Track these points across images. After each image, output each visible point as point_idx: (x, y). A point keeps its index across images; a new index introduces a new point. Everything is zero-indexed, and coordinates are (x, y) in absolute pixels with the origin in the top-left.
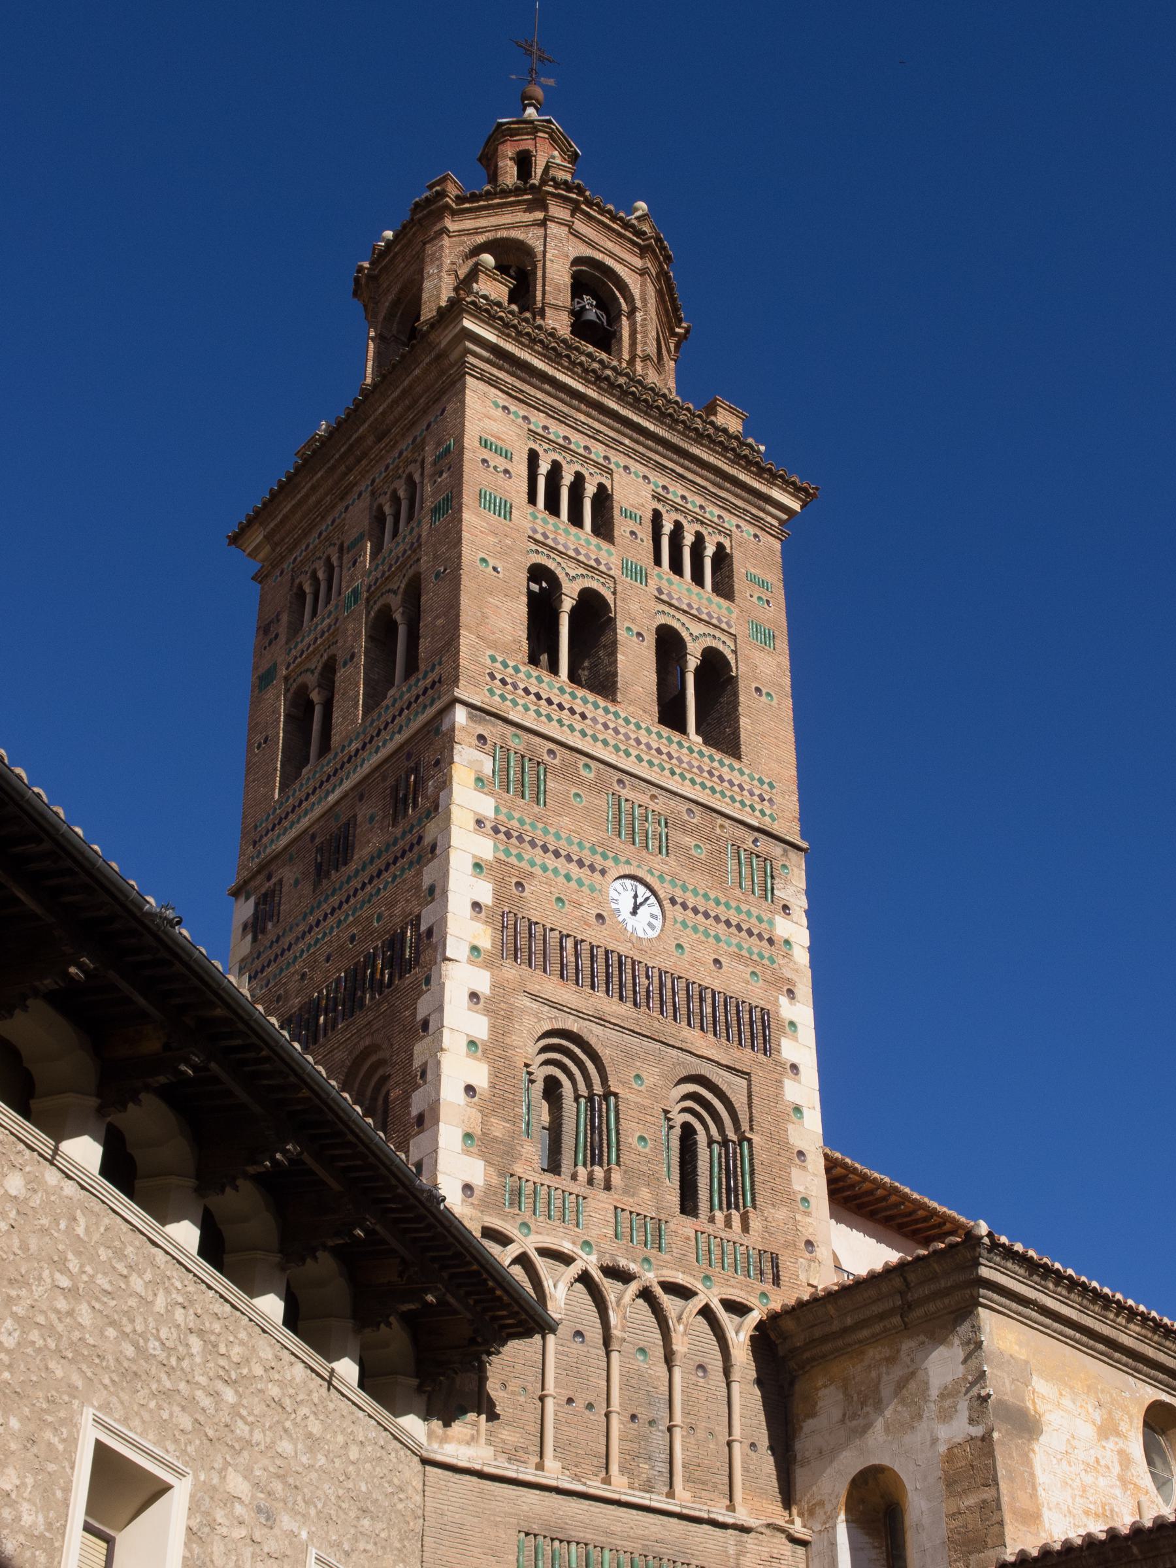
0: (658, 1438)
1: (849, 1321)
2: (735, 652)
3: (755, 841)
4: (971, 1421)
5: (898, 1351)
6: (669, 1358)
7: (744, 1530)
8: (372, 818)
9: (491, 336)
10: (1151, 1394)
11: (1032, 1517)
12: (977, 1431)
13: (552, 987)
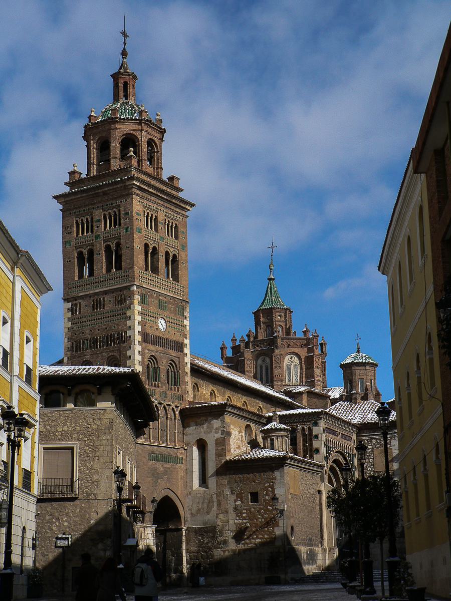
0: (165, 432)
1: (199, 412)
2: (178, 254)
3: (181, 303)
4: (221, 434)
5: (207, 419)
6: (167, 418)
7: (178, 449)
8: (110, 301)
9: (138, 184)
10: (246, 423)
11: (230, 450)
12: (223, 436)
13: (151, 347)
